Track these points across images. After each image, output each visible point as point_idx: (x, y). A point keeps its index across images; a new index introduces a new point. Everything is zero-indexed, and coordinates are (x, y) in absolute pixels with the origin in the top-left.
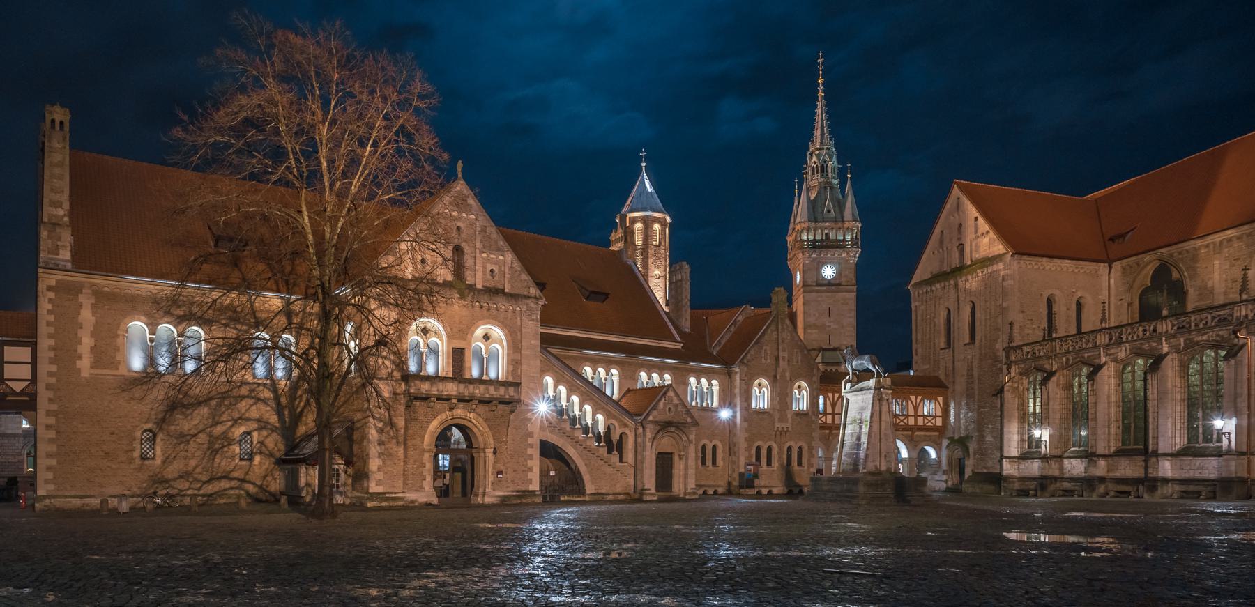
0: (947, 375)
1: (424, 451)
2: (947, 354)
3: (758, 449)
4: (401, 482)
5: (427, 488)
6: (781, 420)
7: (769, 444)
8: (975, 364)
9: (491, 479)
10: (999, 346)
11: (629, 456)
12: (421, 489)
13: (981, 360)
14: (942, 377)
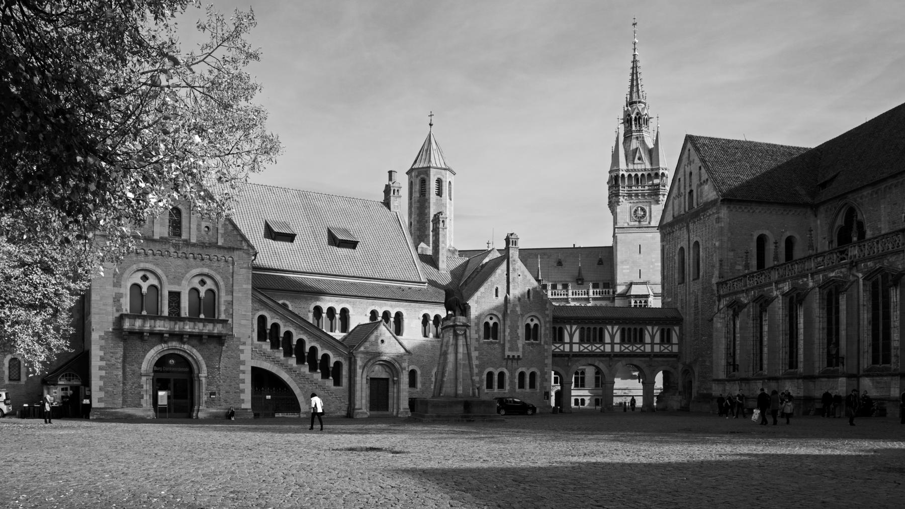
0: (682, 307)
1: (141, 375)
3: (490, 375)
4: (120, 400)
5: (144, 405)
6: (511, 349)
7: (499, 370)
8: (700, 298)
9: (204, 398)
11: (345, 381)
12: (139, 405)
13: (703, 293)
14: (679, 309)
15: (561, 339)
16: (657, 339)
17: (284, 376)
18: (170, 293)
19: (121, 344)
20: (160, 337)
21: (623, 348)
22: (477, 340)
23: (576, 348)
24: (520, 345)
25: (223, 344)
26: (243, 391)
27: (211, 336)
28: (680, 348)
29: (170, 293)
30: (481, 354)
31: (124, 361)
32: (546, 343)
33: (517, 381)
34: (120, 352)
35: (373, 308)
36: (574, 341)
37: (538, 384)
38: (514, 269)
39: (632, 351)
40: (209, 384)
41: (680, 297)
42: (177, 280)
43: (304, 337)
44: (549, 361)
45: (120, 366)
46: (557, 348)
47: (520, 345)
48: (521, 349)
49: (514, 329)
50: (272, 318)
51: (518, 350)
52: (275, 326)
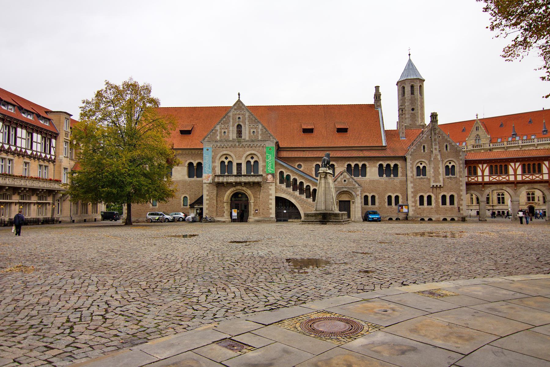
3: (422, 197)
6: (434, 181)
7: (428, 194)
12: (223, 216)
15: (475, 173)
17: (293, 201)
18: (237, 164)
19: (216, 188)
20: (230, 184)
21: (524, 177)
22: (412, 177)
23: (486, 179)
25: (261, 187)
26: (271, 209)
27: (254, 183)
29: (237, 164)
30: (414, 185)
31: (217, 196)
33: (440, 201)
34: (215, 192)
35: (349, 163)
36: (485, 174)
37: (456, 202)
38: (435, 134)
40: (255, 205)
42: (240, 157)
43: (303, 181)
44: (464, 187)
45: (215, 198)
46: (473, 179)
48: (442, 181)
49: (436, 169)
50: (286, 172)
51: (439, 182)
52: (288, 176)
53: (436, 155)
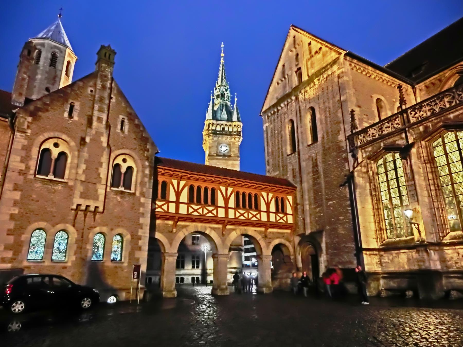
0: (294, 177)
2: (294, 159)
6: (83, 196)
10: (341, 137)
13: (324, 155)
14: (290, 179)
16: (272, 208)
24: (101, 191)
28: (295, 219)
32: (143, 194)
36: (181, 200)
39: (248, 219)
41: (290, 168)
47: (101, 191)
48: (102, 198)
49: (93, 167)
51: (96, 198)
53: (99, 134)
